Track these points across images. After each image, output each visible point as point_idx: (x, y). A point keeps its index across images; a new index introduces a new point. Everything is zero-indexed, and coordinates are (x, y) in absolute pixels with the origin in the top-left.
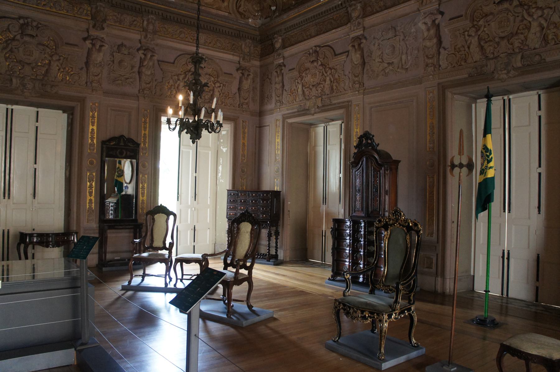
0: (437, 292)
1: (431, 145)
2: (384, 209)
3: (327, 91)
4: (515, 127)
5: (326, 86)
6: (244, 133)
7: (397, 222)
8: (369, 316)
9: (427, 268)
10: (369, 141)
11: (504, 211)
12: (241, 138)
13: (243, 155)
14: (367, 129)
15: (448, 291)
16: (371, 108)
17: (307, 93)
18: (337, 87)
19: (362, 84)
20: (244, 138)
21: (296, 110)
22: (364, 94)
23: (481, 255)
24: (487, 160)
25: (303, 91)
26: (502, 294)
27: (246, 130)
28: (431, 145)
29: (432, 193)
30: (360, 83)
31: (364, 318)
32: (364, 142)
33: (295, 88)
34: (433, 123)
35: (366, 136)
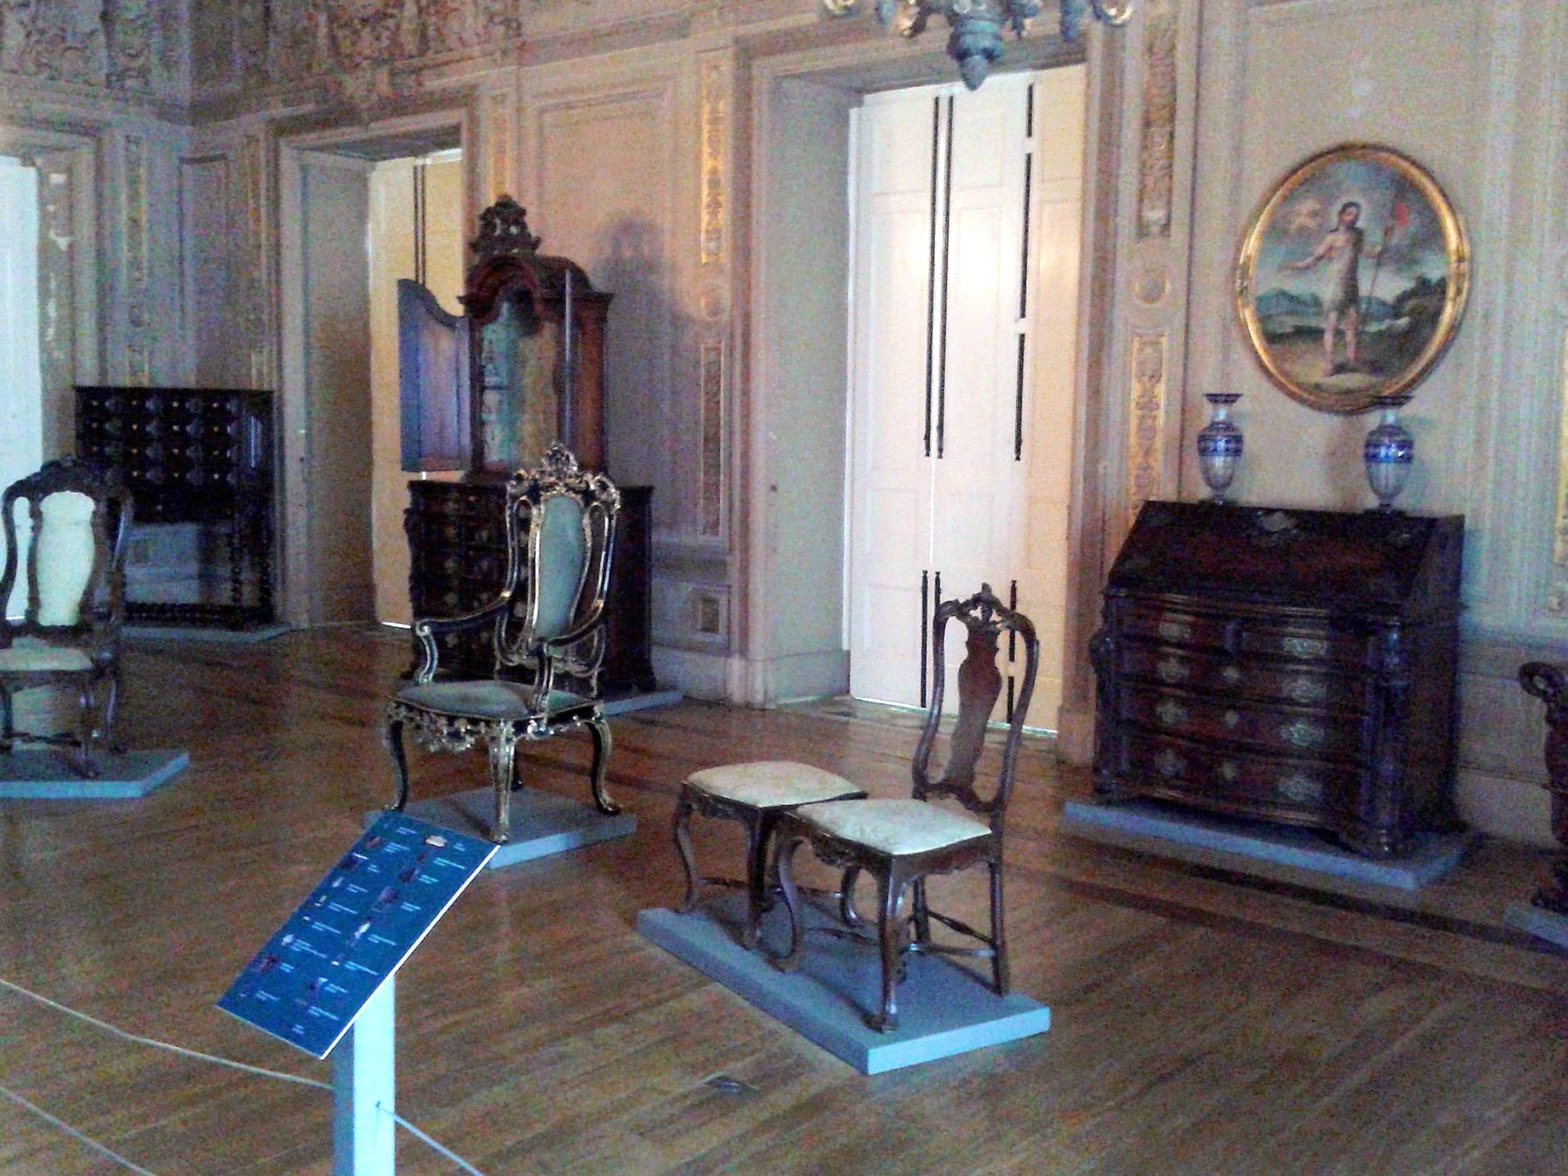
3: (410, 44)
5: (405, 26)
6: (133, 182)
10: (514, 230)
12: (123, 198)
13: (135, 264)
14: (510, 189)
16: (542, 112)
17: (346, 46)
18: (438, 30)
19: (513, 25)
20: (133, 198)
21: (310, 107)
22: (520, 64)
25: (333, 39)
27: (142, 171)
28: (712, 245)
30: (507, 22)
32: (498, 232)
33: (306, 23)
35: (508, 210)
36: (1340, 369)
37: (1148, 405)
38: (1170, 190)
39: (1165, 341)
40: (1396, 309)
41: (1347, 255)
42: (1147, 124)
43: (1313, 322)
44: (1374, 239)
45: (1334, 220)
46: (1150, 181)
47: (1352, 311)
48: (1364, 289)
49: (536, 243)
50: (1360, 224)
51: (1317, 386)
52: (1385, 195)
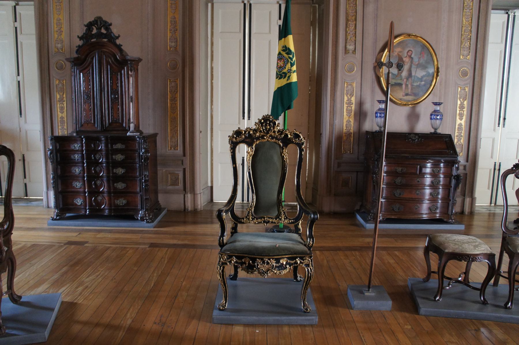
0: (197, 209)
1: (173, 44)
2: (129, 120)
4: (255, 33)
7: (268, 133)
8: (287, 263)
9: (171, 185)
11: (244, 119)
15: (199, 207)
23: (219, 164)
24: (291, 62)
26: (243, 200)
28: (173, 44)
29: (174, 99)
31: (282, 267)
34: (175, 18)
35: (99, 23)
36: (407, 95)
37: (350, 103)
38: (355, 41)
39: (354, 85)
40: (421, 80)
41: (409, 64)
42: (347, 20)
43: (399, 81)
44: (416, 60)
45: (406, 55)
46: (349, 38)
47: (410, 79)
48: (413, 74)
49: (118, 37)
50: (412, 56)
51: (401, 99)
52: (419, 49)
